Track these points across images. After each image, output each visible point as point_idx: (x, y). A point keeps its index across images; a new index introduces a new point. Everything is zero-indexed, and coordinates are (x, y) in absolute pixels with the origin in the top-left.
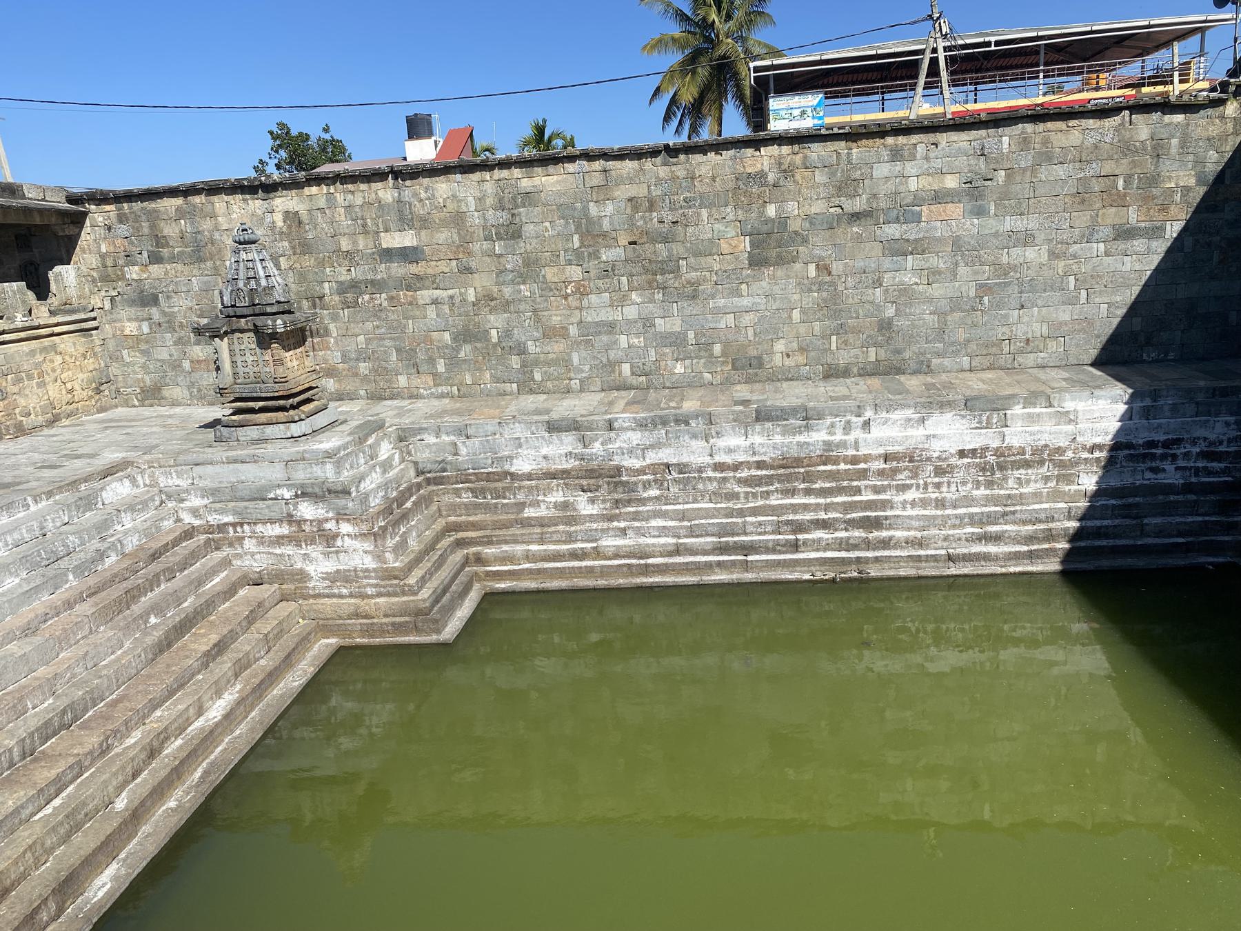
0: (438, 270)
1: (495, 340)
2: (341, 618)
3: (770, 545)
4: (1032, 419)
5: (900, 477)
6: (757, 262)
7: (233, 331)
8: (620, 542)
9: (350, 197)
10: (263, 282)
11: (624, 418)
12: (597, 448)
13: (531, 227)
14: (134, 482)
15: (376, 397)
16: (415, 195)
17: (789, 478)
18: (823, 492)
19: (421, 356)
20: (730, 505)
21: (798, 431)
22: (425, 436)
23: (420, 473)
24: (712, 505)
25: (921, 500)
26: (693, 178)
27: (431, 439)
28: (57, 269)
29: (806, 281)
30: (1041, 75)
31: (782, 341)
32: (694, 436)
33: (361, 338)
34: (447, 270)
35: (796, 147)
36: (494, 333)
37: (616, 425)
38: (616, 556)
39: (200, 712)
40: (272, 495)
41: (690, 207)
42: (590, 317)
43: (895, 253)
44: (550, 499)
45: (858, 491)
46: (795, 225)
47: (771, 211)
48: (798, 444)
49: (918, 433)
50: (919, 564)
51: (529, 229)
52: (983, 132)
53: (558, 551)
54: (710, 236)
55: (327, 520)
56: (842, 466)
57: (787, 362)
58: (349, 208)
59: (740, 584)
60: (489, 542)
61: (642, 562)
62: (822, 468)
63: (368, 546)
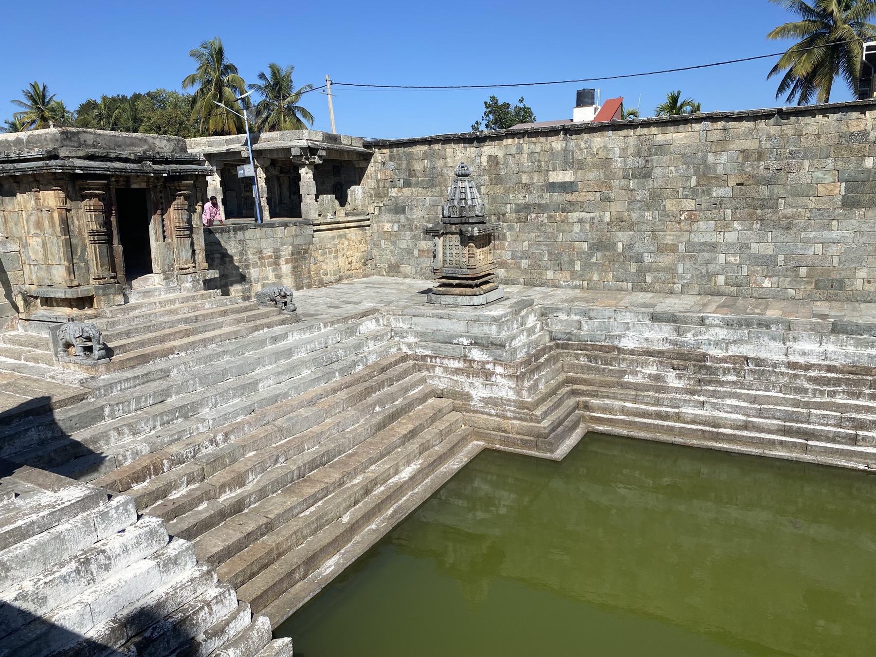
0: (586, 199)
1: (620, 250)
2: (488, 429)
3: (831, 435)
6: (850, 203)
7: (447, 233)
9: (532, 146)
10: (470, 202)
11: (714, 317)
12: (689, 337)
13: (660, 170)
15: (530, 284)
16: (577, 145)
17: (856, 383)
19: (565, 258)
20: (798, 397)
22: (559, 314)
23: (552, 339)
24: (781, 395)
26: (800, 136)
27: (563, 317)
28: (353, 188)
31: (865, 269)
32: (773, 338)
33: (526, 243)
34: (592, 199)
36: (620, 245)
37: (707, 322)
38: (693, 422)
39: (397, 472)
40: (456, 341)
41: (794, 158)
42: (696, 238)
44: (647, 371)
48: (869, 356)
51: (658, 172)
53: (647, 411)
54: (809, 181)
55: (488, 362)
57: (867, 287)
59: (797, 462)
60: (595, 395)
61: (714, 430)
63: (512, 384)
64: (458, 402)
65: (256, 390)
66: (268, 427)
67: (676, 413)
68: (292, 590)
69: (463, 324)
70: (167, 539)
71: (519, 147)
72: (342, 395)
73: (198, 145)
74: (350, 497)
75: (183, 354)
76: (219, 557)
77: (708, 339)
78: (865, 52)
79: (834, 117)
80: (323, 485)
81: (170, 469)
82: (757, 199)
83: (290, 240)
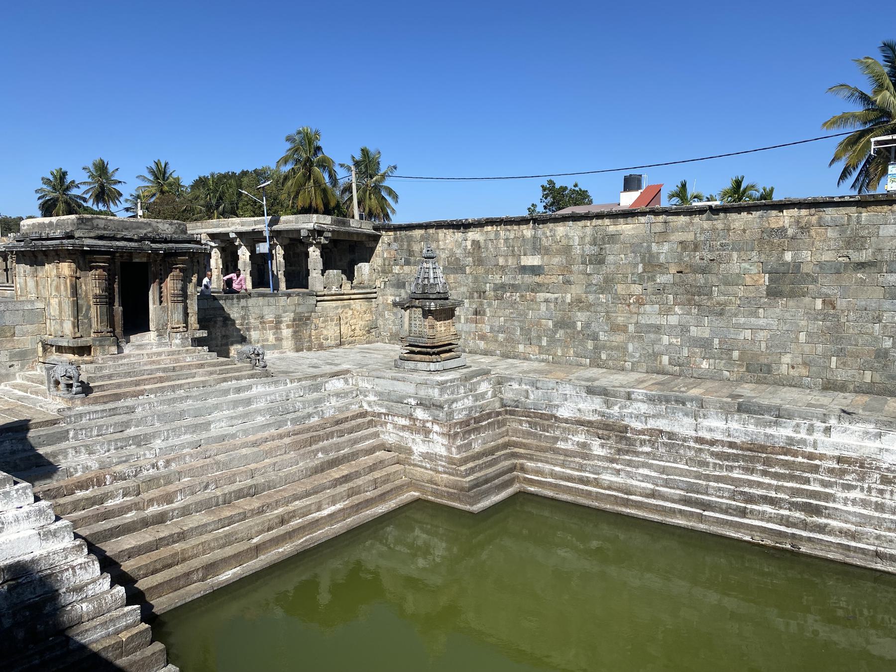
1: (579, 329)
3: (724, 507)
5: (847, 477)
6: (773, 293)
7: (412, 307)
8: (614, 479)
9: (508, 233)
10: (432, 281)
11: (639, 392)
14: (346, 381)
15: (505, 356)
16: (544, 233)
17: (752, 459)
18: (776, 476)
19: (533, 334)
21: (769, 424)
22: (512, 383)
23: (503, 405)
24: (686, 467)
25: (862, 500)
26: (729, 230)
27: (516, 386)
28: (360, 265)
29: (813, 312)
31: (789, 355)
32: (686, 414)
33: (502, 319)
35: (813, 211)
36: (579, 324)
37: (633, 396)
38: (609, 488)
39: (319, 509)
40: (406, 401)
41: (724, 250)
42: (643, 320)
44: (576, 439)
45: (807, 481)
46: (805, 269)
47: (788, 256)
49: (876, 444)
50: (848, 553)
51: (610, 259)
53: (572, 475)
54: (737, 271)
55: (428, 421)
56: (800, 459)
58: (506, 240)
59: (692, 531)
60: (531, 458)
61: (626, 496)
62: (782, 457)
63: (445, 441)
64: (402, 456)
65: (208, 430)
66: (208, 460)
67: (595, 479)
68: (188, 588)
69: (413, 385)
70: (54, 518)
71: (497, 232)
72: (287, 440)
73: (233, 224)
74: (263, 523)
75: (152, 396)
76: (129, 553)
77: (631, 413)
78: (873, 147)
79: (756, 214)
80: (241, 511)
81: (111, 483)
82: (695, 286)
83: (293, 308)
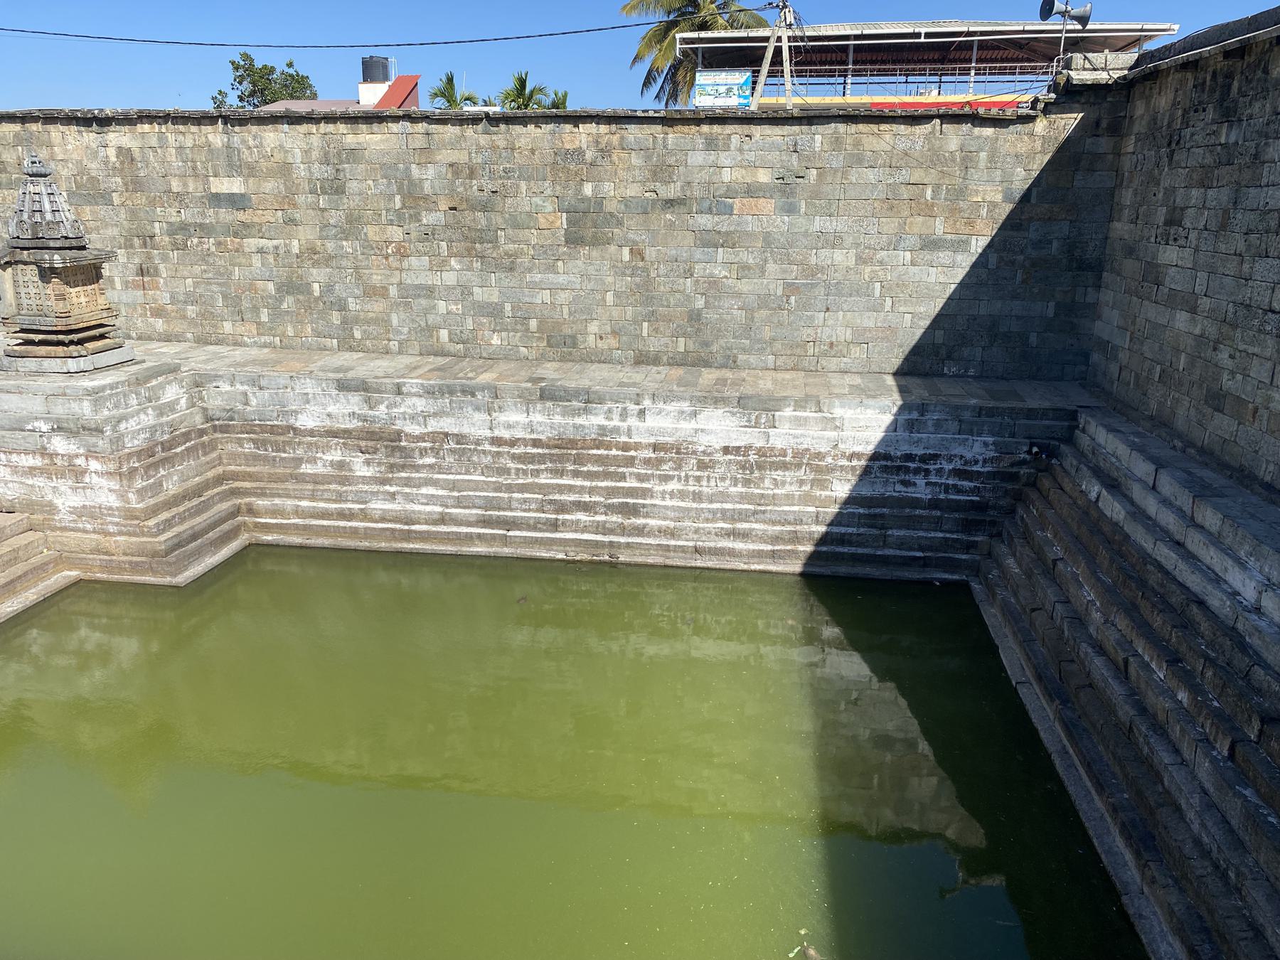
0: (264, 219)
1: (317, 294)
2: (84, 552)
3: (532, 522)
4: (799, 422)
6: (574, 240)
7: (17, 263)
8: (389, 506)
9: (181, 138)
10: (49, 217)
11: (412, 383)
15: (202, 341)
16: (244, 142)
17: (561, 459)
18: (590, 476)
19: (246, 304)
20: (500, 480)
21: (576, 413)
23: (209, 419)
24: (483, 478)
26: (513, 149)
27: (226, 387)
30: (973, 72)
32: (477, 409)
34: (273, 220)
35: (614, 127)
36: (316, 286)
37: (404, 389)
38: (383, 520)
40: (30, 427)
41: (509, 178)
42: (410, 279)
43: (706, 244)
44: (328, 457)
45: (623, 477)
46: (611, 206)
47: (588, 189)
48: (574, 426)
51: (353, 186)
52: (796, 128)
53: (327, 509)
54: (528, 209)
55: (77, 456)
56: (614, 452)
57: (600, 344)
58: (180, 149)
60: (262, 494)
61: (406, 527)
63: (114, 485)
64: (38, 517)
77: (404, 413)
78: (678, 46)
82: (475, 228)
